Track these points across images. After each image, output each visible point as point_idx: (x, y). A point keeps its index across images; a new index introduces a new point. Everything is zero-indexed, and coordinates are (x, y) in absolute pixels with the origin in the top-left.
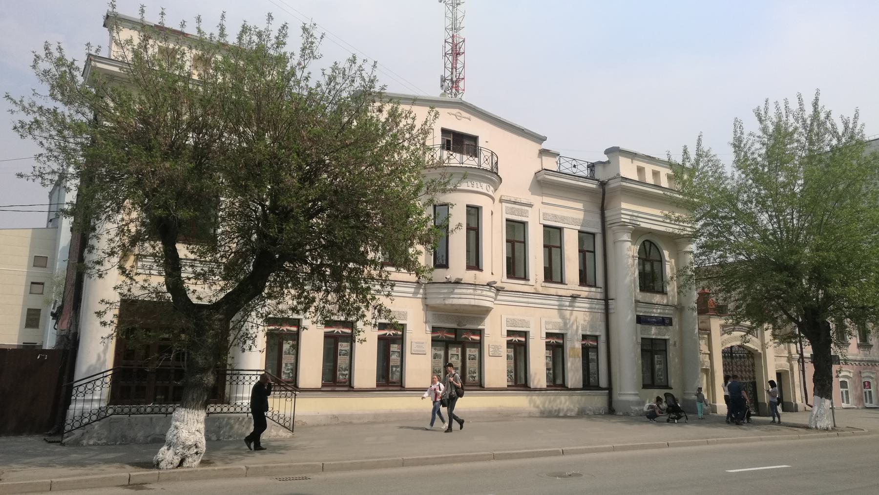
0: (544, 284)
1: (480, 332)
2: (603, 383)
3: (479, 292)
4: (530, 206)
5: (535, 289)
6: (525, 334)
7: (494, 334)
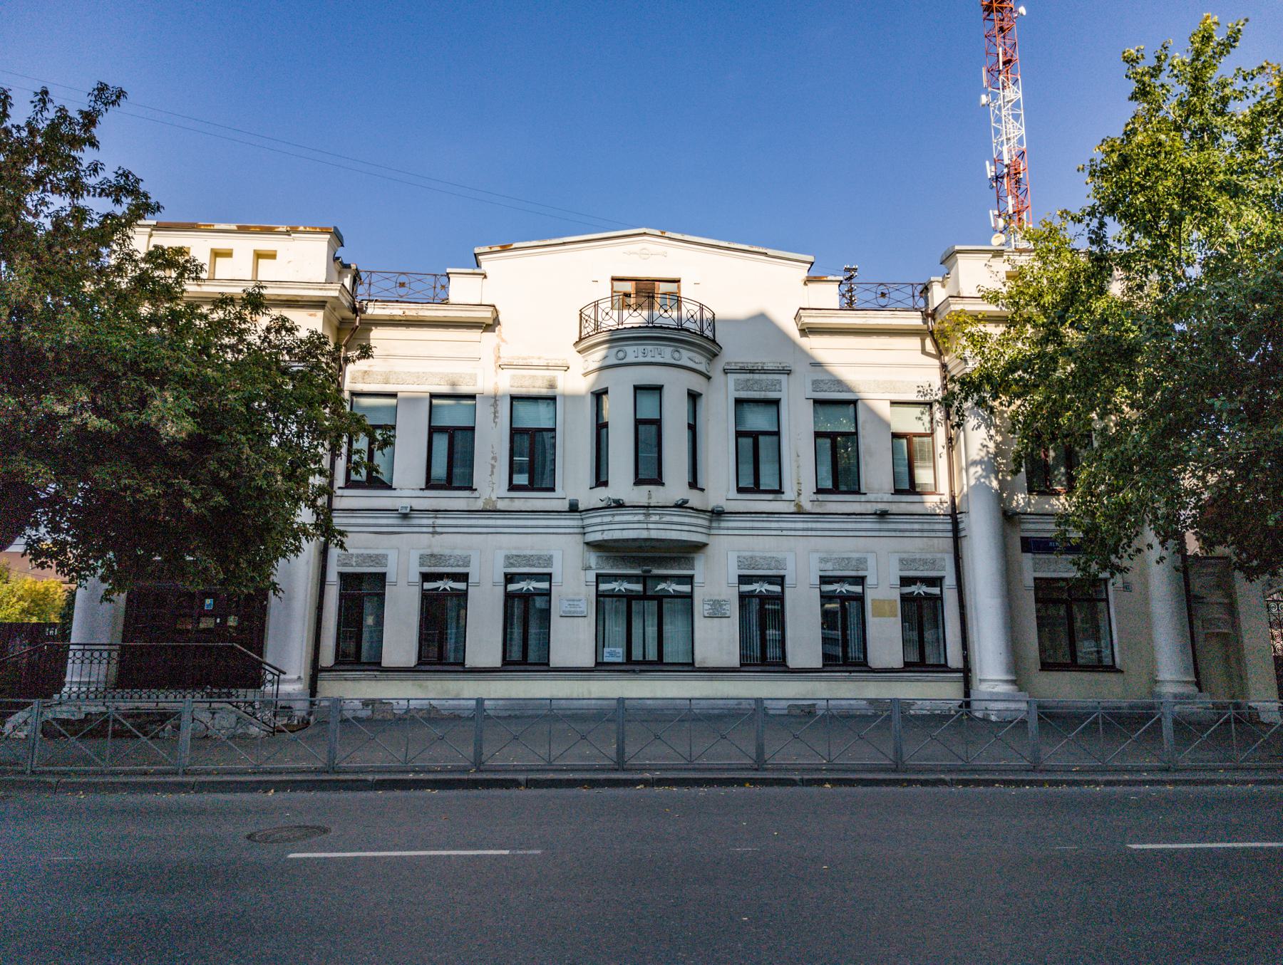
0: (814, 497)
1: (689, 580)
2: (954, 659)
3: (654, 518)
4: (789, 372)
5: (798, 505)
6: (780, 580)
7: (716, 580)
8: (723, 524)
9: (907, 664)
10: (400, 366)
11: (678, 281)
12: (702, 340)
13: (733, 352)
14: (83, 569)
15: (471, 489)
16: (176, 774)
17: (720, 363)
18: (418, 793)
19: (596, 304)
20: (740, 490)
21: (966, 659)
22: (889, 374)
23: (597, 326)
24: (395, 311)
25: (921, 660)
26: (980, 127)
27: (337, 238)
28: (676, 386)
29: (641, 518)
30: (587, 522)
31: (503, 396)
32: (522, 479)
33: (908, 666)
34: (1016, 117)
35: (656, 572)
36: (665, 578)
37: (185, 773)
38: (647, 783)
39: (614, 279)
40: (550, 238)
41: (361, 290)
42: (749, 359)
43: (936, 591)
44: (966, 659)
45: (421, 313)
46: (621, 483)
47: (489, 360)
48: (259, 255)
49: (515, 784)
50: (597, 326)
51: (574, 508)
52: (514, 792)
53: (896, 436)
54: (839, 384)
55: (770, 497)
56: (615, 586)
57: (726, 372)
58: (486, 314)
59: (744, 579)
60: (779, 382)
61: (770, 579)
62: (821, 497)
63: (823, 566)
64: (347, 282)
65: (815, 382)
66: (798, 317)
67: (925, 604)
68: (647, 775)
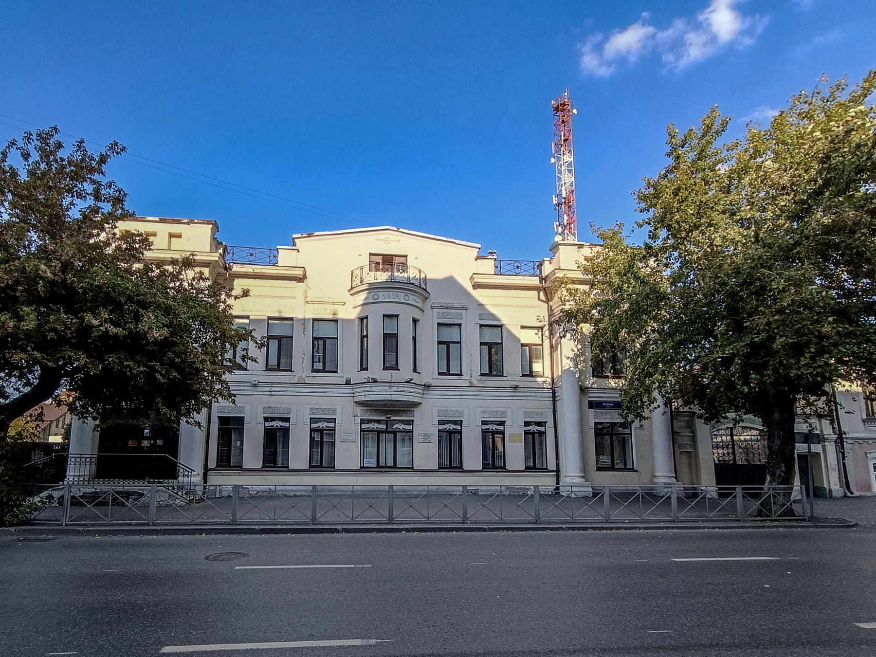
0: (480, 378)
1: (411, 422)
2: (552, 466)
5: (470, 382)
6: (460, 423)
7: (426, 423)
8: (430, 392)
9: (526, 468)
10: (255, 303)
11: (406, 256)
12: (420, 289)
13: (435, 298)
14: (85, 413)
15: (291, 371)
16: (148, 525)
17: (429, 303)
18: (284, 535)
19: (361, 268)
20: (440, 374)
21: (558, 465)
22: (519, 313)
23: (362, 281)
24: (248, 269)
25: (534, 465)
26: (551, 176)
27: (216, 228)
28: (406, 315)
29: (387, 388)
30: (355, 390)
31: (309, 319)
32: (319, 366)
33: (528, 469)
34: (570, 171)
35: (393, 418)
36: (400, 421)
37: (154, 525)
38: (407, 530)
39: (371, 254)
40: (336, 230)
41: (227, 257)
42: (444, 301)
43: (543, 429)
44: (558, 465)
45: (263, 271)
46: (375, 369)
47: (300, 299)
48: (171, 236)
49: (336, 531)
50: (362, 281)
51: (348, 383)
52: (335, 535)
53: (523, 345)
54: (493, 317)
55: (456, 377)
56: (371, 426)
57: (432, 308)
58: (299, 273)
59: (441, 423)
60: (461, 314)
61: (455, 422)
62: (482, 377)
63: (483, 415)
64: (221, 251)
65: (480, 315)
66: (471, 278)
67: (537, 435)
68: (406, 526)
